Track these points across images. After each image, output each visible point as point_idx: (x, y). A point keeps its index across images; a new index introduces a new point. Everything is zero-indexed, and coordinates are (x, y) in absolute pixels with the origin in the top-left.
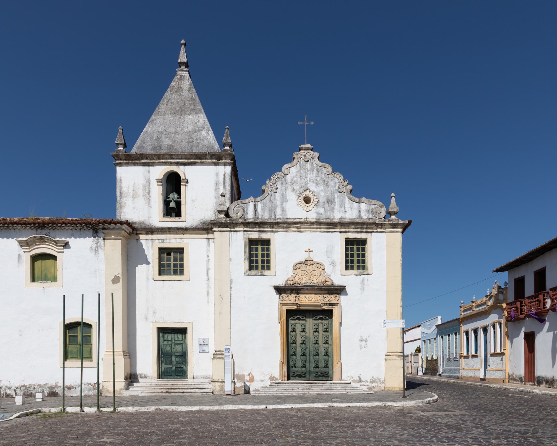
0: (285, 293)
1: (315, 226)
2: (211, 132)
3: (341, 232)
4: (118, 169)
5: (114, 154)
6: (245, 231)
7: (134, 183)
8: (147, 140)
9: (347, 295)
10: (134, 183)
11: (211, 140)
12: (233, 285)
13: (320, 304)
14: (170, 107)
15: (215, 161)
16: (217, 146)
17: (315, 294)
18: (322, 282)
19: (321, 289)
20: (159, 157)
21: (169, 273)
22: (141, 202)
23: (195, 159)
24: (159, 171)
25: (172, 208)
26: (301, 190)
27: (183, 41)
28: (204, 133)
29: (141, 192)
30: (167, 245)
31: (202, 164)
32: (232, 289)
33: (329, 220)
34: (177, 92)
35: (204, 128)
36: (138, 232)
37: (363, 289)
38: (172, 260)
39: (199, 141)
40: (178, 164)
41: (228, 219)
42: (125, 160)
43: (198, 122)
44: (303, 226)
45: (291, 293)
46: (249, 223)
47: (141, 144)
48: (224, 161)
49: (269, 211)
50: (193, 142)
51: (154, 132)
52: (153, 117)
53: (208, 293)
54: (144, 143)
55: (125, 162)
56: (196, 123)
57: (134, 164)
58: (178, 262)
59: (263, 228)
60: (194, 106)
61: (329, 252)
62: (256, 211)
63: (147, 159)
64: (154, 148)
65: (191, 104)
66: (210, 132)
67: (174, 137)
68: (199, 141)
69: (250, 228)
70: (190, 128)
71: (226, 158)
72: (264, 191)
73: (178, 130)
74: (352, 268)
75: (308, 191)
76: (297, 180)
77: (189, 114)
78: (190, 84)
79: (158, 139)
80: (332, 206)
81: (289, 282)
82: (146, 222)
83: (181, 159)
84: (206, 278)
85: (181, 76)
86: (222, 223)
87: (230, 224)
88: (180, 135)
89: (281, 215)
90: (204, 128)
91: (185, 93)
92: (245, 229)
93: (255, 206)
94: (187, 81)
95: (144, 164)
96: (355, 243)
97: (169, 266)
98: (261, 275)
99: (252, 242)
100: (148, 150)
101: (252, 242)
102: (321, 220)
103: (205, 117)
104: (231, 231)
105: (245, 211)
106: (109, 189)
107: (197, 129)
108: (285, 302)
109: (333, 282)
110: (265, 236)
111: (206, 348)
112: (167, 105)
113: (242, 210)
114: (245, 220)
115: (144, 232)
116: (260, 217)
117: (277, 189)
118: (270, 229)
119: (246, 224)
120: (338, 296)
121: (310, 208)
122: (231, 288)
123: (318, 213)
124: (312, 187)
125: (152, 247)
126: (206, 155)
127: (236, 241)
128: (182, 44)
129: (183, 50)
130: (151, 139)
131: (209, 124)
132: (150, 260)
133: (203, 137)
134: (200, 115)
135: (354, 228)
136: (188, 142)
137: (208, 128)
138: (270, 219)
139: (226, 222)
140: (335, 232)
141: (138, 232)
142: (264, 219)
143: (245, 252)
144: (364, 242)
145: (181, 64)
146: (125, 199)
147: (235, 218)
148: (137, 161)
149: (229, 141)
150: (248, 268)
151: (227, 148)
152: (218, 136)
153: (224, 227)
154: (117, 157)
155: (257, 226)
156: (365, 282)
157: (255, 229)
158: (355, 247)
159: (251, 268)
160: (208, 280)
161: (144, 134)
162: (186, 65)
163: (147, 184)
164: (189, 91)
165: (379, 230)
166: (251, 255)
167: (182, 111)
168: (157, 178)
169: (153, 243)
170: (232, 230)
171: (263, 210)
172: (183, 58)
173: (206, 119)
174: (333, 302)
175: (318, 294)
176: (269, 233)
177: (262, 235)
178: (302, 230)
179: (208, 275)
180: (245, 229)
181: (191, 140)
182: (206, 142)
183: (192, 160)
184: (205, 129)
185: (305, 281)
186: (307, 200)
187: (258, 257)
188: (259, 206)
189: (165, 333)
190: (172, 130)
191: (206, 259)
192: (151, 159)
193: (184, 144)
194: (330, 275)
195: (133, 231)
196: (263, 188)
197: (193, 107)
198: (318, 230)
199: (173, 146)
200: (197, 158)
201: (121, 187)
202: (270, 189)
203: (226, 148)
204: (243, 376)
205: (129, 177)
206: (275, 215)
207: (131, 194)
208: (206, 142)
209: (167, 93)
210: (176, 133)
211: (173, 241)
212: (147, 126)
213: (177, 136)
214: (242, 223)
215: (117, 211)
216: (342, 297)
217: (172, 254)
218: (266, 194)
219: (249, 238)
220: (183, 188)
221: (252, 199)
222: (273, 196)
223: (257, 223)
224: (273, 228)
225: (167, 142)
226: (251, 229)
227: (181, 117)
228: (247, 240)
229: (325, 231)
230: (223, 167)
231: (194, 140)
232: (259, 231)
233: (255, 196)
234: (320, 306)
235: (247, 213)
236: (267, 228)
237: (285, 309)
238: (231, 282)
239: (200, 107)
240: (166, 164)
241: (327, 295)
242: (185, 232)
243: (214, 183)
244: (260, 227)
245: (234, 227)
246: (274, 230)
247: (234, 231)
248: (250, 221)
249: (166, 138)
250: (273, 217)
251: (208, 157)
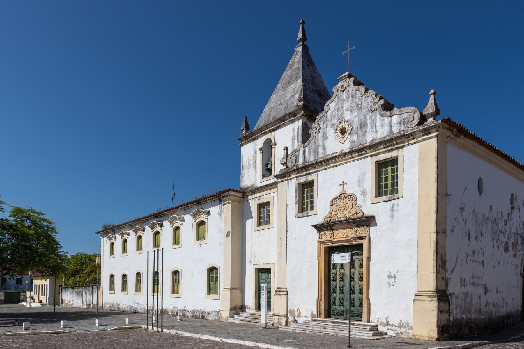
0: (323, 230)
1: (348, 157)
3: (372, 156)
6: (297, 177)
9: (376, 225)
12: (288, 229)
13: (349, 238)
17: (347, 228)
18: (353, 215)
19: (349, 222)
26: (338, 122)
32: (288, 232)
33: (361, 146)
36: (248, 194)
37: (392, 216)
44: (338, 160)
45: (327, 230)
59: (309, 170)
61: (361, 181)
62: (304, 155)
69: (300, 173)
74: (386, 194)
75: (344, 121)
76: (335, 114)
80: (364, 129)
81: (326, 220)
89: (322, 154)
96: (389, 164)
102: (354, 149)
104: (288, 180)
108: (323, 240)
109: (363, 213)
110: (310, 178)
115: (250, 194)
116: (307, 161)
117: (320, 129)
118: (313, 170)
120: (367, 228)
121: (345, 139)
123: (352, 142)
124: (347, 116)
132: (253, 215)
135: (384, 148)
140: (366, 157)
141: (248, 194)
144: (394, 162)
156: (395, 208)
158: (389, 168)
165: (411, 142)
171: (309, 153)
174: (361, 235)
175: (349, 228)
178: (338, 163)
185: (340, 216)
186: (343, 132)
188: (307, 149)
189: (262, 273)
194: (361, 206)
195: (245, 194)
198: (352, 159)
204: (294, 311)
206: (318, 155)
216: (372, 228)
219: (299, 183)
222: (317, 137)
229: (357, 160)
232: (306, 175)
234: (350, 241)
236: (311, 169)
237: (323, 246)
241: (357, 228)
244: (307, 171)
245: (290, 176)
246: (317, 170)
247: (290, 179)
248: (300, 166)
250: (317, 158)
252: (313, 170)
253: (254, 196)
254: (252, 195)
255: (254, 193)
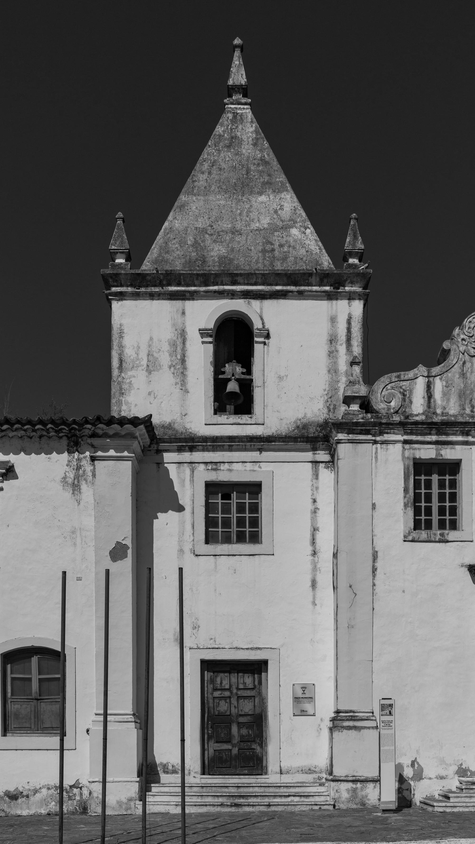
2: (310, 231)
4: (116, 305)
5: (108, 271)
6: (406, 442)
7: (151, 339)
8: (174, 245)
10: (151, 339)
11: (313, 248)
14: (217, 177)
15: (327, 288)
16: (326, 262)
20: (207, 279)
21: (227, 540)
22: (165, 380)
23: (284, 285)
24: (205, 313)
25: (233, 394)
27: (237, 41)
28: (294, 231)
29: (165, 359)
30: (223, 476)
31: (301, 295)
34: (229, 147)
35: (295, 222)
38: (234, 508)
39: (286, 249)
40: (247, 295)
41: (369, 415)
42: (131, 285)
43: (282, 208)
46: (416, 423)
47: (160, 255)
48: (347, 289)
49: (460, 397)
50: (273, 250)
51: (186, 229)
52: (183, 198)
53: (314, 584)
54: (167, 252)
55: (130, 289)
56: (276, 212)
57: (152, 296)
58: (247, 515)
59: (447, 434)
60: (269, 175)
63: (179, 285)
64: (190, 262)
65: (261, 172)
66: (308, 231)
67: (232, 240)
68: (286, 249)
69: (417, 434)
70: (265, 221)
71: (352, 283)
72: (446, 354)
73: (239, 226)
77: (260, 193)
78: (256, 132)
79: (196, 244)
82: (176, 426)
83: (255, 284)
84: (309, 549)
85: (235, 115)
86: (357, 424)
87: (374, 424)
88: (244, 238)
90: (295, 222)
91: (247, 149)
92: (406, 437)
93: (429, 387)
94: (249, 125)
95: (173, 296)
97: (227, 523)
98: (440, 541)
99: (420, 468)
100: (178, 266)
101: (420, 468)
103: (295, 199)
104: (375, 442)
105: (406, 397)
106: (94, 350)
107: (280, 224)
110: (449, 454)
111: (308, 707)
112: (210, 173)
113: (401, 396)
114: (407, 417)
116: (439, 411)
118: (460, 438)
119: (409, 426)
122: (374, 570)
125: (192, 481)
126: (311, 275)
127: (384, 468)
128: (236, 46)
129: (237, 60)
130: (182, 243)
131: (304, 214)
133: (295, 241)
134: (283, 196)
136: (264, 251)
137: (304, 221)
138: (462, 415)
139: (364, 421)
141: (163, 446)
142: (447, 414)
143: (406, 490)
145: (231, 91)
146: (130, 373)
147: (384, 412)
148: (157, 289)
149: (360, 245)
150: (412, 525)
151: (353, 261)
152: (330, 237)
153: (360, 434)
154: (116, 279)
155: (434, 432)
157: (428, 438)
159: (417, 525)
160: (314, 553)
161: (166, 234)
162: (244, 91)
163: (179, 342)
164: (255, 145)
166: (417, 498)
167: (243, 186)
168: (202, 327)
169: (193, 471)
170: (378, 439)
171: (445, 395)
172: (238, 76)
173: (297, 204)
176: (458, 447)
177: (443, 452)
179: (313, 542)
180: (406, 437)
181: (268, 247)
182: (303, 252)
183: (279, 288)
184: (298, 225)
187: (431, 502)
190: (227, 225)
191: (310, 507)
192: (188, 285)
193: (255, 254)
195: (151, 443)
196: (446, 345)
197: (267, 178)
199: (231, 260)
200: (291, 282)
201: (121, 346)
202: (462, 348)
203: (351, 261)
205: (139, 324)
207: (144, 362)
208: (303, 252)
209: (207, 150)
210: (235, 232)
211: (238, 468)
212: (170, 217)
213: (237, 239)
214: (402, 424)
215: (113, 401)
217: (234, 495)
218: (452, 358)
219: (414, 459)
220: (258, 348)
221: (422, 369)
222: (468, 365)
223: (435, 424)
224: (468, 434)
225: (216, 251)
226: (419, 438)
227: (241, 197)
228: (411, 463)
230: (345, 302)
231: (276, 246)
232: (437, 443)
233: (429, 365)
235: (411, 402)
238: (375, 557)
239: (281, 178)
240: (220, 295)
242: (266, 445)
243: (325, 338)
244: (438, 434)
245: (381, 433)
247: (383, 442)
248: (417, 418)
249: (215, 241)
250: (468, 411)
251: (313, 280)
252: (460, 438)
253: (186, 456)
254: (180, 450)
255: (192, 449)
